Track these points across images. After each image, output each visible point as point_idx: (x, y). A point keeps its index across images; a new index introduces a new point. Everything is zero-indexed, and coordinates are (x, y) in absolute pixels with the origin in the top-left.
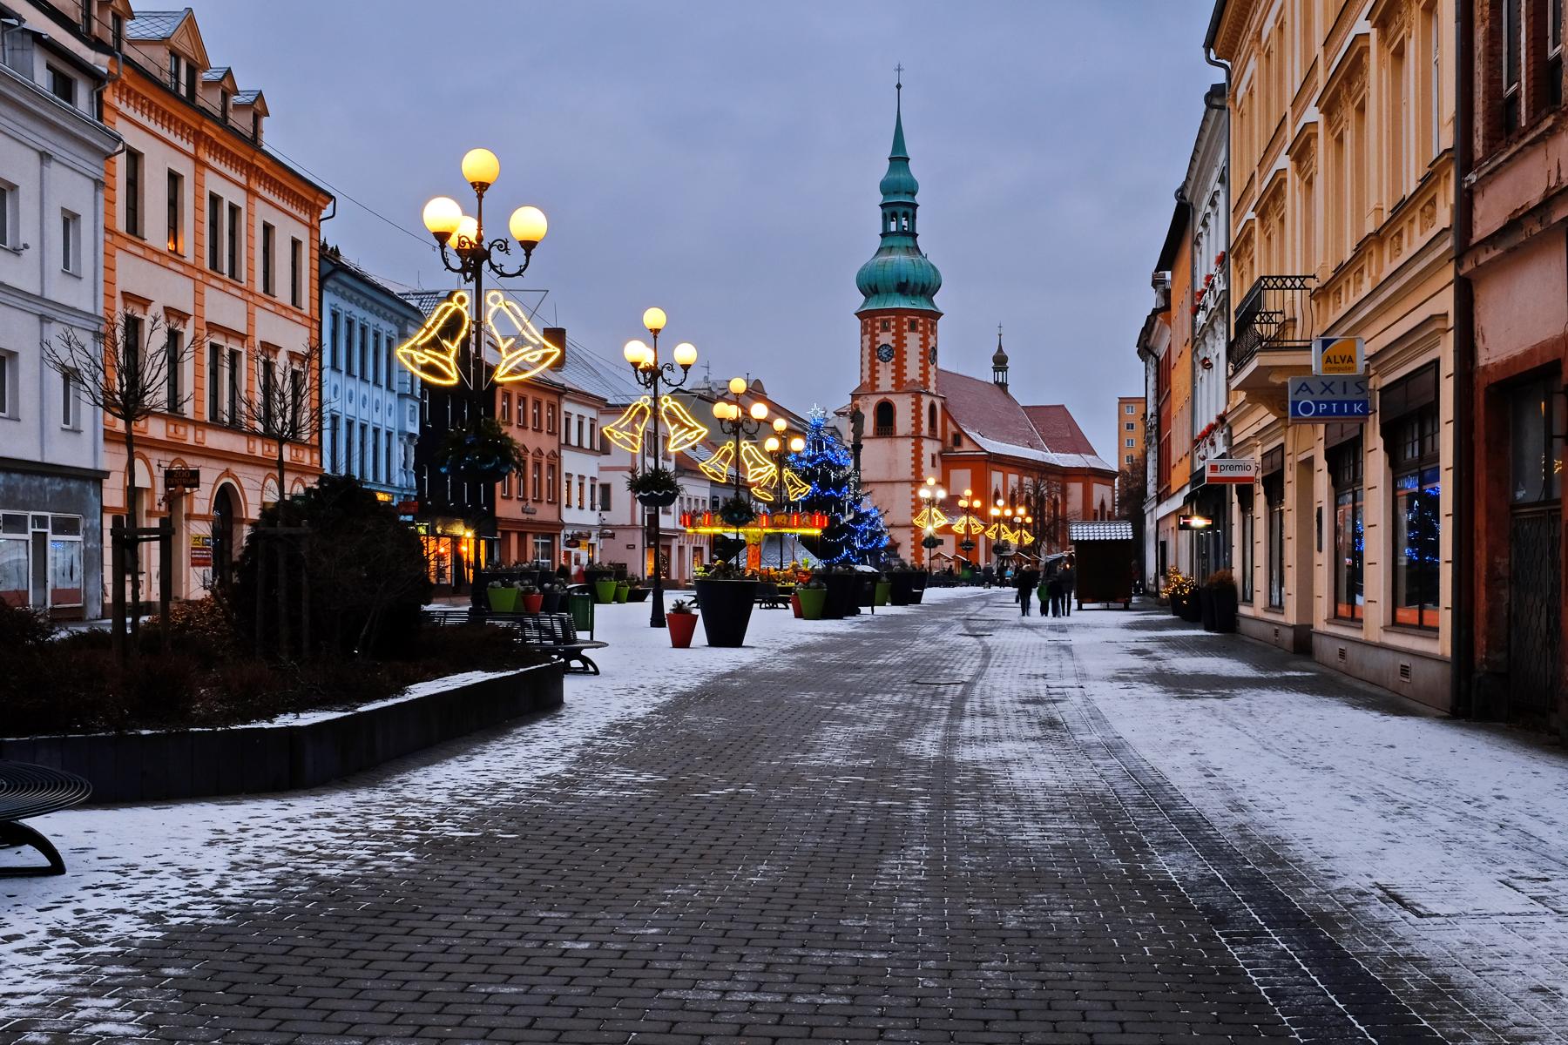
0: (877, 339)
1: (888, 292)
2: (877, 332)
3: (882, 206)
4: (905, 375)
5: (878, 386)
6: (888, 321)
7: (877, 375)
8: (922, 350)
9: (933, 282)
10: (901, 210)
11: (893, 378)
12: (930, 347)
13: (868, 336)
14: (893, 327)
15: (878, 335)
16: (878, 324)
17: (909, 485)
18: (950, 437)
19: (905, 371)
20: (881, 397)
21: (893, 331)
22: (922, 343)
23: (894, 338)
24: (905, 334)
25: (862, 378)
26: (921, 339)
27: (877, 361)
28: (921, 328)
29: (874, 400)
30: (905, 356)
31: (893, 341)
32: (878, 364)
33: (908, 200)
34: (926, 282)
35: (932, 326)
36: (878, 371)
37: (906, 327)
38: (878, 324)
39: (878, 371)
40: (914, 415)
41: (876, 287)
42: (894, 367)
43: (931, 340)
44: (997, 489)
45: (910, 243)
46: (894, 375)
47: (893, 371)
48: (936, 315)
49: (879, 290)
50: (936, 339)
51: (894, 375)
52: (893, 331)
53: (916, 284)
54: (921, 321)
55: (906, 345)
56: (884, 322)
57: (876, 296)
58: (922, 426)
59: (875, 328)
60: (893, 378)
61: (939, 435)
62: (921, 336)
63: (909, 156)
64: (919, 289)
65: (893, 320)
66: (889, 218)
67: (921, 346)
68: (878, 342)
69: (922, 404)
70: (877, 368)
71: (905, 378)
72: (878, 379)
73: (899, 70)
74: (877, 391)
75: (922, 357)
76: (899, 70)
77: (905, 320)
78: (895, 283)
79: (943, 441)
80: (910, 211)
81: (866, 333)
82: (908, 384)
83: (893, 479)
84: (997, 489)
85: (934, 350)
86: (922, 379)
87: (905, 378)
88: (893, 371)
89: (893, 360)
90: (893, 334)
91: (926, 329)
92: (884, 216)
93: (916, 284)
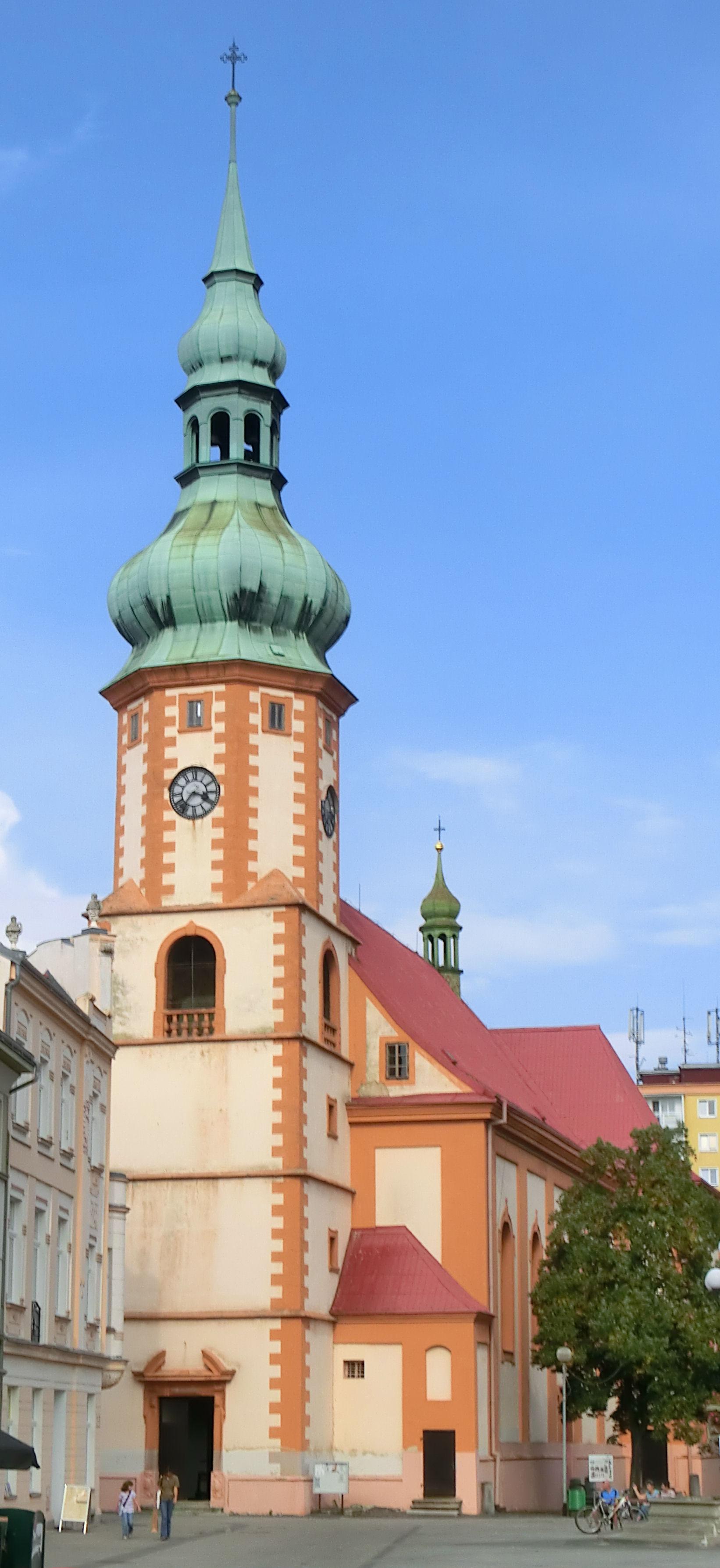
0: (169, 753)
1: (203, 617)
2: (170, 732)
4: (254, 856)
5: (170, 890)
7: (167, 858)
8: (301, 788)
9: (331, 601)
11: (215, 865)
12: (323, 785)
13: (143, 748)
14: (219, 717)
15: (172, 742)
16: (172, 711)
17: (264, 1187)
18: (375, 1057)
21: (219, 727)
22: (300, 768)
23: (221, 748)
26: (297, 757)
27: (170, 815)
28: (298, 726)
30: (253, 802)
31: (218, 759)
32: (171, 826)
33: (260, 377)
34: (316, 605)
36: (171, 847)
37: (256, 719)
38: (172, 711)
39: (171, 847)
42: (220, 833)
43: (326, 763)
46: (219, 855)
47: (216, 844)
49: (177, 620)
50: (336, 766)
51: (219, 855)
53: (285, 599)
54: (299, 704)
55: (255, 771)
56: (192, 703)
57: (168, 633)
59: (159, 721)
60: (215, 865)
62: (300, 747)
64: (294, 615)
65: (220, 696)
67: (298, 777)
68: (173, 763)
70: (168, 837)
71: (252, 866)
72: (171, 868)
73: (234, 58)
74: (167, 902)
75: (301, 809)
76: (234, 58)
77: (255, 696)
78: (228, 590)
80: (265, 410)
81: (135, 740)
82: (259, 884)
83: (214, 1167)
84: (506, 1214)
85: (332, 792)
86: (300, 872)
87: (252, 866)
88: (216, 844)
89: (219, 812)
90: (218, 738)
92: (194, 424)
93: (285, 599)
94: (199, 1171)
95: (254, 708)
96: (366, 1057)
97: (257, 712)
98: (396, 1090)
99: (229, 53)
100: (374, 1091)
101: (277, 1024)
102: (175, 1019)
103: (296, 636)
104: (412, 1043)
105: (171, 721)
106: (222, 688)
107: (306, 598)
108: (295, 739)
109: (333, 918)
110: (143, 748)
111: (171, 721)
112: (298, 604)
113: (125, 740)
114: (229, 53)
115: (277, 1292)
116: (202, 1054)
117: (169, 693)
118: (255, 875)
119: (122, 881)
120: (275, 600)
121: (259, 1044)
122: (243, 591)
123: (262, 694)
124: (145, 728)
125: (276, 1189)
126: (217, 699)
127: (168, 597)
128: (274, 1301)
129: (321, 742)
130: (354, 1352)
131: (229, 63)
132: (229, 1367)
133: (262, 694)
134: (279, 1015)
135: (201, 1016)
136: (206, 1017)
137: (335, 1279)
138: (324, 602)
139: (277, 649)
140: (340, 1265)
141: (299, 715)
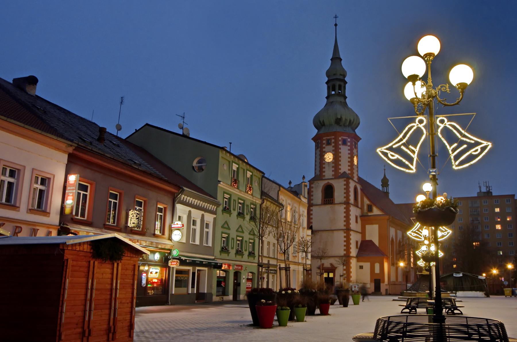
2: (324, 146)
3: (327, 83)
4: (340, 169)
6: (330, 139)
7: (324, 170)
10: (337, 83)
11: (333, 171)
13: (319, 149)
14: (333, 143)
15: (324, 148)
16: (324, 142)
18: (366, 207)
19: (340, 167)
20: (326, 182)
21: (333, 144)
22: (349, 152)
23: (334, 148)
24: (340, 147)
25: (315, 173)
26: (349, 150)
28: (349, 144)
29: (322, 184)
30: (340, 159)
33: (341, 77)
34: (352, 120)
35: (355, 143)
37: (340, 143)
38: (324, 142)
40: (345, 191)
41: (323, 121)
44: (392, 238)
45: (342, 100)
46: (333, 169)
48: (358, 139)
50: (357, 151)
51: (333, 169)
52: (333, 144)
53: (346, 120)
54: (349, 140)
55: (340, 153)
57: (323, 127)
58: (350, 198)
59: (322, 144)
60: (333, 171)
61: (360, 206)
62: (349, 148)
63: (341, 57)
64: (348, 124)
65: (333, 139)
66: (331, 88)
69: (350, 185)
71: (340, 171)
72: (324, 172)
73: (336, 17)
74: (323, 178)
76: (336, 17)
77: (340, 138)
79: (362, 209)
80: (342, 84)
81: (318, 148)
84: (392, 238)
86: (350, 172)
87: (340, 171)
88: (333, 167)
90: (333, 147)
91: (351, 146)
92: (328, 88)
93: (346, 120)
94: (330, 229)
95: (340, 141)
96: (364, 208)
97: (340, 141)
98: (370, 214)
99: (335, 16)
100: (365, 214)
101: (345, 201)
102: (325, 201)
103: (349, 127)
104: (373, 205)
105: (324, 144)
106: (334, 137)
107: (350, 119)
108: (348, 146)
109: (357, 181)
110: (319, 149)
111: (324, 144)
112: (349, 121)
113: (316, 148)
114: (335, 16)
115: (345, 252)
116: (331, 207)
117: (324, 138)
118: (340, 173)
119: (316, 174)
120: (344, 119)
121: (341, 205)
122: (337, 118)
123: (342, 138)
124: (320, 145)
125: (345, 233)
126: (333, 139)
127: (323, 120)
128: (344, 254)
129: (354, 147)
130: (361, 264)
131: (335, 18)
132: (336, 267)
133: (342, 138)
134: (345, 199)
135: (330, 200)
136: (331, 200)
137: (357, 250)
138: (354, 120)
139: (344, 129)
140: (359, 247)
141: (349, 142)
